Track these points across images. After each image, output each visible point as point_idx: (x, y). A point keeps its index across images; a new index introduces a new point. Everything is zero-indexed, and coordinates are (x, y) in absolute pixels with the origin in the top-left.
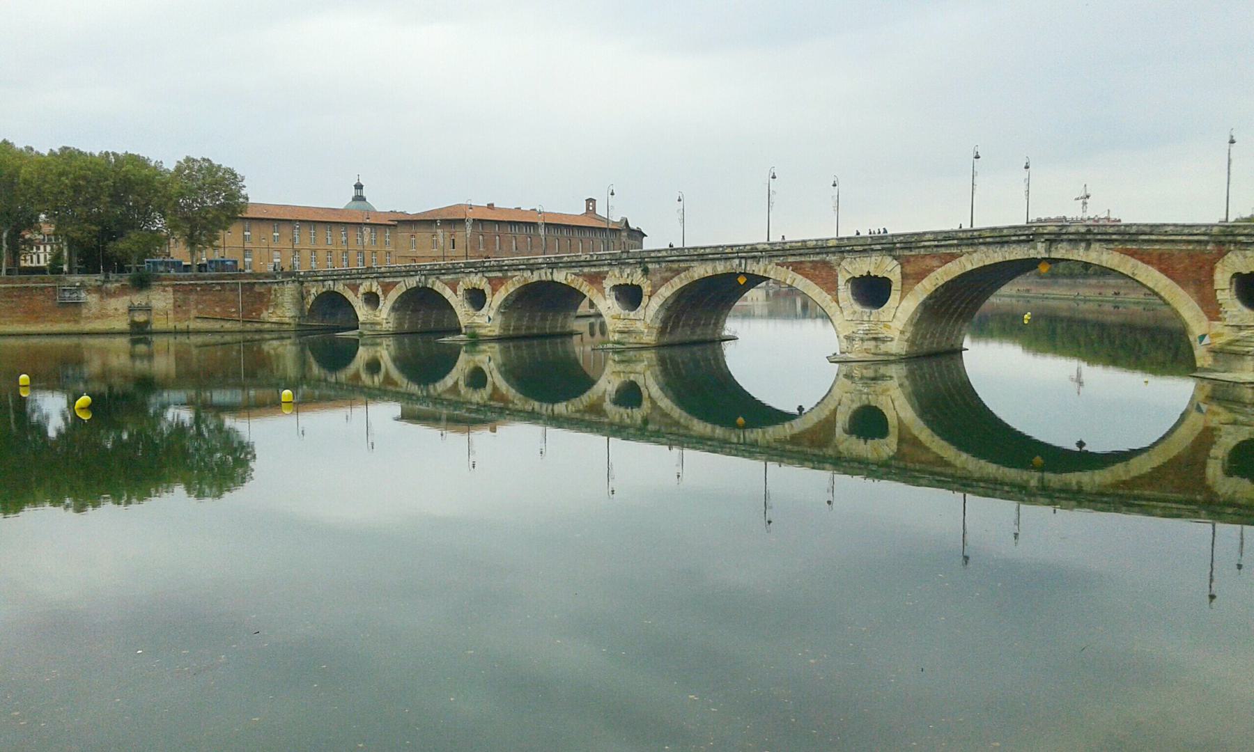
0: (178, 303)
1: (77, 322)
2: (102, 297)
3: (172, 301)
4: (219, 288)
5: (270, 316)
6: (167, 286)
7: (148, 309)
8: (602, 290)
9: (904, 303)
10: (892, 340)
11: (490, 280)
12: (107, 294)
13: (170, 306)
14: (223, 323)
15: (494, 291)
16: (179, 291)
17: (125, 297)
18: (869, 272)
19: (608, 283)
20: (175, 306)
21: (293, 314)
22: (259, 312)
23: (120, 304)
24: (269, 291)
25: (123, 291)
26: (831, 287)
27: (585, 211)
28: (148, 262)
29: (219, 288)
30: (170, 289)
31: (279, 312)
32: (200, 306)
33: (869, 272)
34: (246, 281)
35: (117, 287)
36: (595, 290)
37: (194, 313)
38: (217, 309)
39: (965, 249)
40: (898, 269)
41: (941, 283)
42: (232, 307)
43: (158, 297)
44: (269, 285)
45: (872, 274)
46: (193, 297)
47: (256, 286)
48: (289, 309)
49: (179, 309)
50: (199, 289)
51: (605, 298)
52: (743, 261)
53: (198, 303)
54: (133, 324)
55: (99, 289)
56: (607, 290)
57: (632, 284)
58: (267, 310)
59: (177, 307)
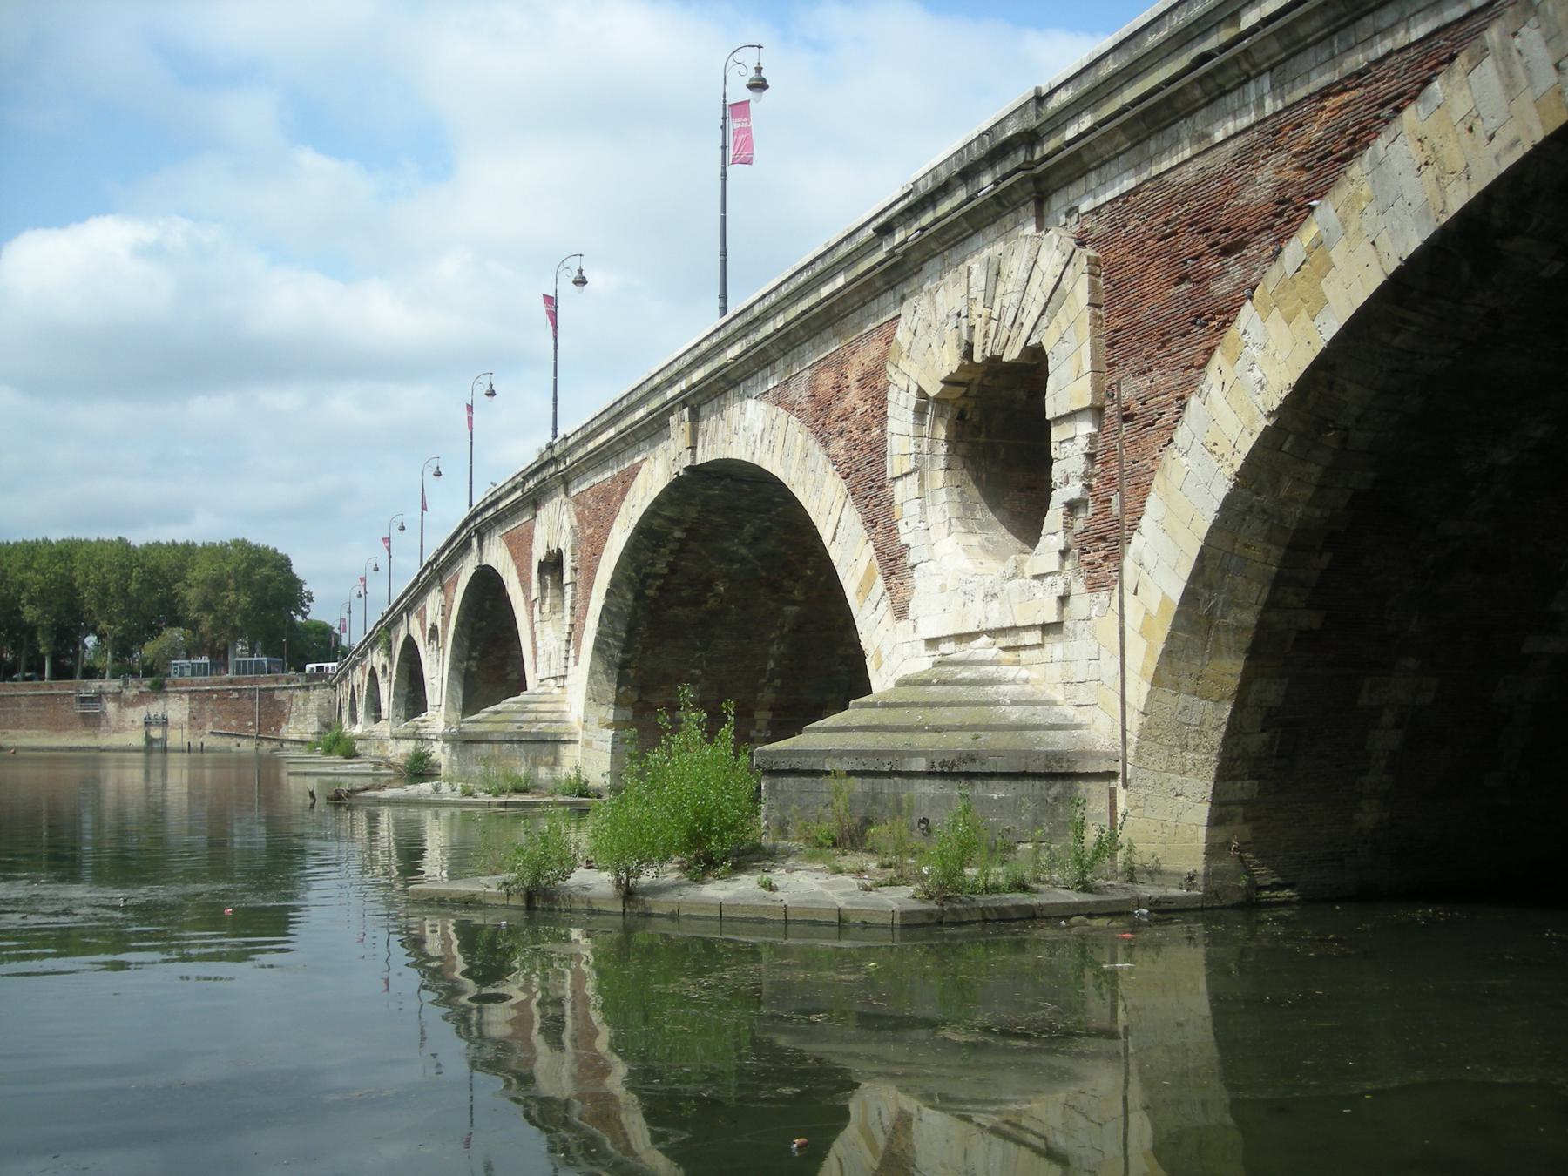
0: (193, 715)
1: (95, 736)
2: (120, 707)
3: (187, 712)
4: (235, 695)
5: (291, 731)
6: (185, 692)
7: (164, 722)
12: (125, 703)
13: (186, 718)
14: (239, 740)
16: (196, 700)
17: (142, 707)
20: (189, 717)
21: (316, 730)
22: (278, 726)
23: (137, 714)
24: (291, 698)
25: (141, 699)
28: (175, 664)
29: (235, 695)
30: (186, 697)
31: (300, 726)
32: (216, 719)
34: (264, 686)
35: (136, 695)
37: (209, 728)
38: (234, 722)
42: (249, 720)
43: (174, 706)
44: (290, 691)
46: (209, 707)
47: (276, 692)
48: (313, 723)
49: (193, 721)
50: (215, 696)
53: (213, 716)
54: (150, 740)
55: (117, 697)
58: (287, 723)
59: (193, 718)
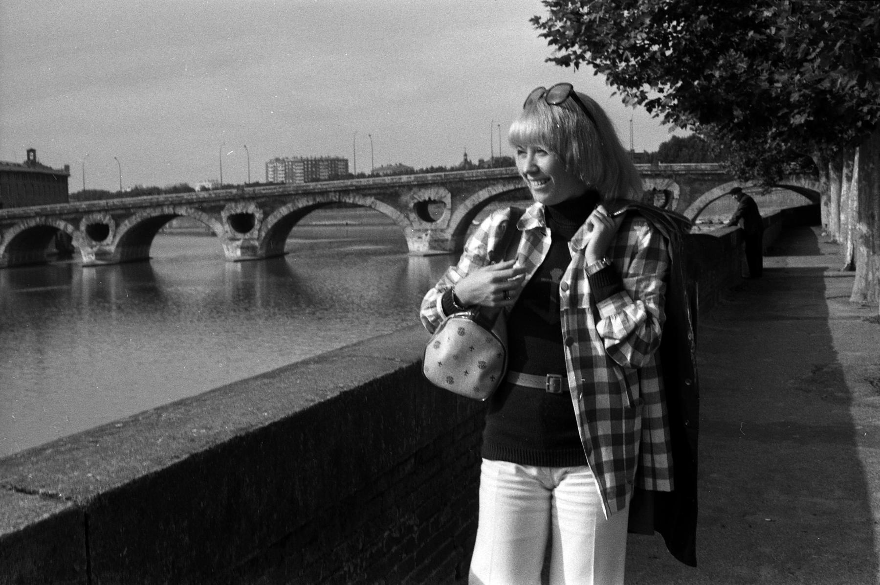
8: (220, 220)
9: (454, 216)
10: (447, 240)
11: (113, 217)
15: (117, 225)
18: (430, 198)
19: (224, 215)
26: (402, 208)
27: (26, 158)
33: (430, 198)
36: (214, 220)
39: (491, 182)
40: (449, 195)
41: (477, 203)
45: (432, 199)
51: (222, 223)
52: (338, 194)
56: (224, 220)
57: (247, 214)
